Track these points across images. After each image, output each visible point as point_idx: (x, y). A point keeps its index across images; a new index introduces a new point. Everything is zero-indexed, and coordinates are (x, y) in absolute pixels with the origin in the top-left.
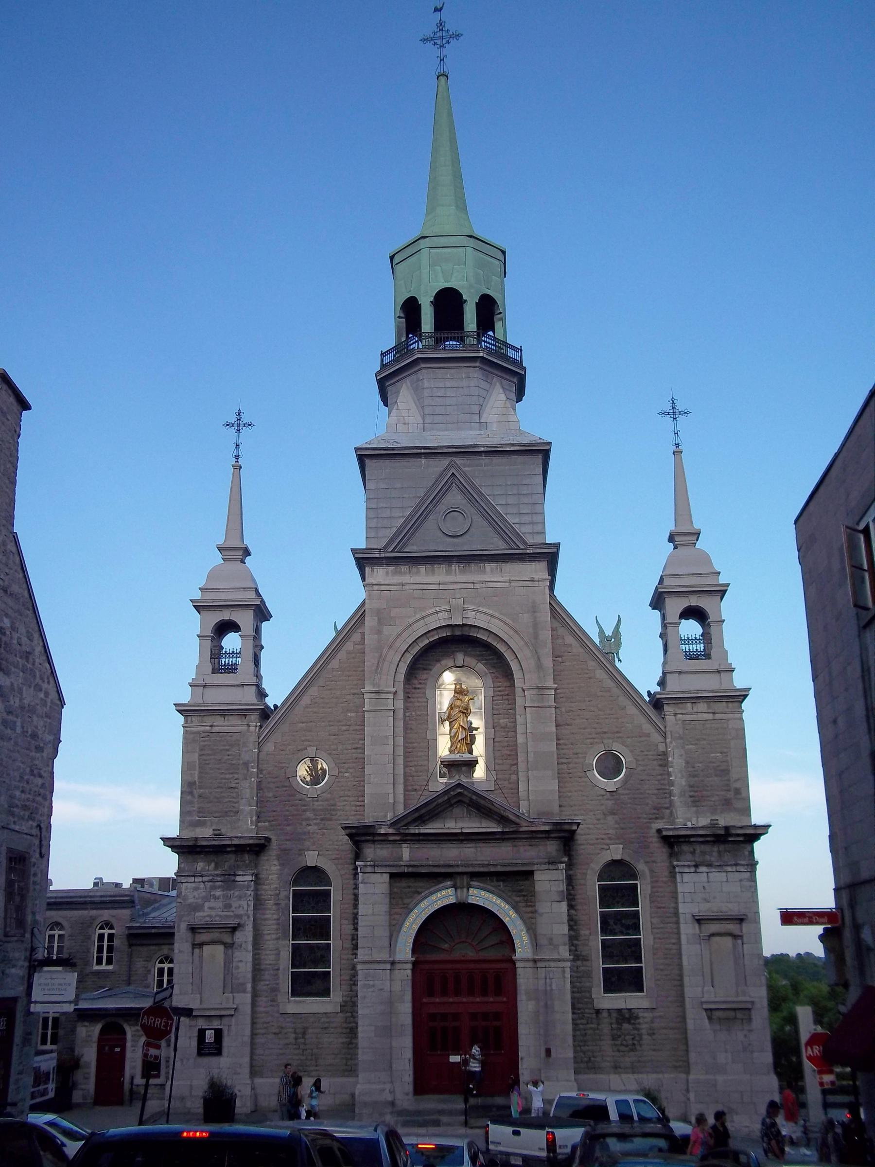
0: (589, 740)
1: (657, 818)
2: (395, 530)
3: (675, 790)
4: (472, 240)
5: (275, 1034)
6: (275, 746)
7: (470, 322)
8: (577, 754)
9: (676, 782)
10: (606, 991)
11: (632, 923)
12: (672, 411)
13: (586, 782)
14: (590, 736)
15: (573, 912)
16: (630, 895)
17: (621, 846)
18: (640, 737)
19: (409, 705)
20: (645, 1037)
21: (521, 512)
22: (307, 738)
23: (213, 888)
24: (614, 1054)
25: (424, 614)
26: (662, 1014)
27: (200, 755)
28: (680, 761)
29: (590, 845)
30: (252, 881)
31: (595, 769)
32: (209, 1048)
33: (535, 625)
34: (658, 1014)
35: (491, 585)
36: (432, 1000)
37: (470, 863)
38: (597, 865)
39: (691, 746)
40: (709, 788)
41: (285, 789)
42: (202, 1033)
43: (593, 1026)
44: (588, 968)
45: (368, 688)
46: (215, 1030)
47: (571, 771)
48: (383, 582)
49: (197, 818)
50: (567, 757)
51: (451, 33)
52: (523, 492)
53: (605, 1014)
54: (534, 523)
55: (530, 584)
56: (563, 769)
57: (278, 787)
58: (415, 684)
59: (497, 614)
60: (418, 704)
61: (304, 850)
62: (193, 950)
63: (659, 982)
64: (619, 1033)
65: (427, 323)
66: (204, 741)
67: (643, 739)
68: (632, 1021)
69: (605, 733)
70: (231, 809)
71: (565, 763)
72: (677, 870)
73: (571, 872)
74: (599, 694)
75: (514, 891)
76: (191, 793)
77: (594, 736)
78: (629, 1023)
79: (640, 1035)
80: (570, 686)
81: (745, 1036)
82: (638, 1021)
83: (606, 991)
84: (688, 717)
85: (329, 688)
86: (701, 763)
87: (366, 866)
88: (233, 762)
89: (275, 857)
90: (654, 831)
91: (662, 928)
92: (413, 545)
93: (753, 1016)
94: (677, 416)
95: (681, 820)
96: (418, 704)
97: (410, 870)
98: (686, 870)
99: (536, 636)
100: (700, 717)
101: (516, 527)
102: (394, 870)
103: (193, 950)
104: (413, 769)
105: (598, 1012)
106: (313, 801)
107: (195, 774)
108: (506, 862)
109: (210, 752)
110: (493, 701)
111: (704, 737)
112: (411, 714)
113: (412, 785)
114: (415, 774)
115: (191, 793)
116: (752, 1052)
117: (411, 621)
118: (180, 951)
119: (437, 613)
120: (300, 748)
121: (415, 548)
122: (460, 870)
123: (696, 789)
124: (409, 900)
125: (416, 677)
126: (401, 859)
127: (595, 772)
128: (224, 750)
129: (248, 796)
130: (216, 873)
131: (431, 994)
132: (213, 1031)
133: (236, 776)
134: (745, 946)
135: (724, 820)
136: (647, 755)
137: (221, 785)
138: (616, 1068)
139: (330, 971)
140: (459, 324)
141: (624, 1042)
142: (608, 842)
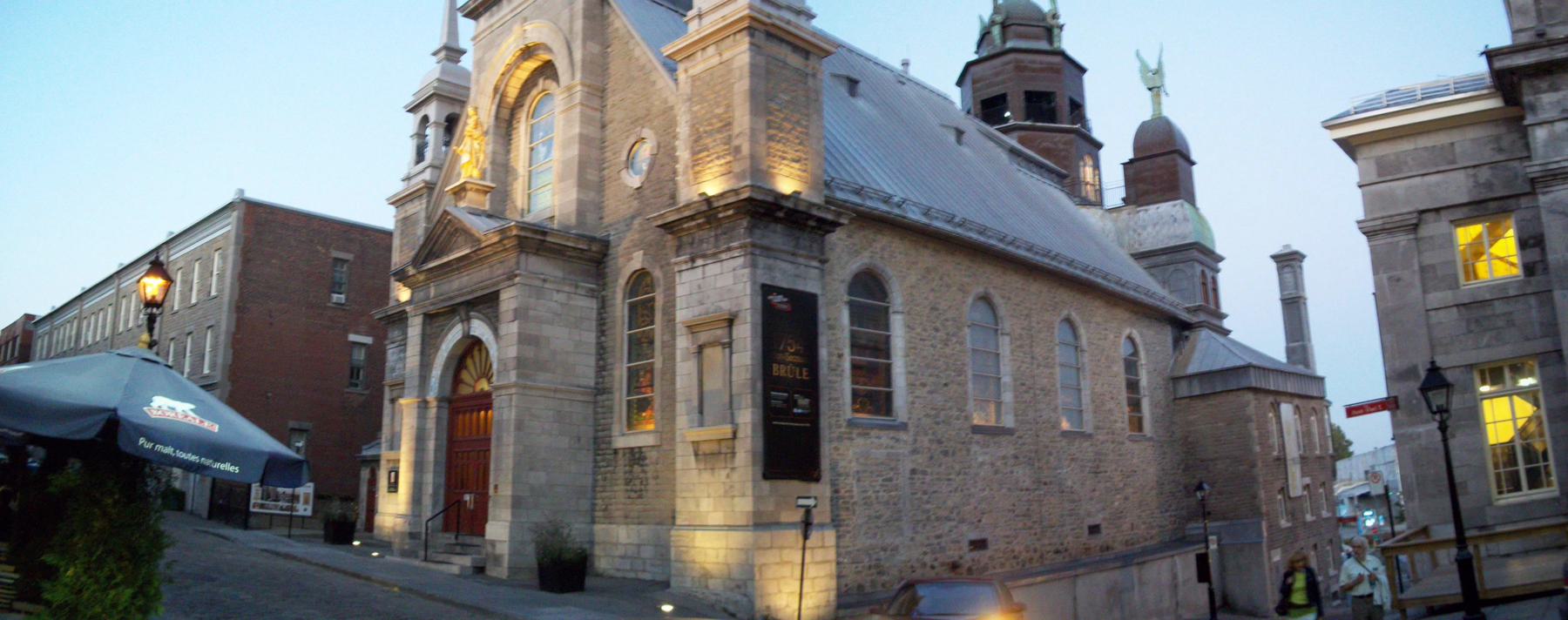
3: (680, 167)
15: (603, 339)
17: (641, 252)
20: (651, 481)
73: (603, 293)
78: (638, 464)
79: (647, 479)
81: (728, 476)
93: (737, 450)
98: (684, 267)
105: (616, 451)
116: (733, 497)
126: (428, 298)
134: (734, 356)
138: (627, 519)
141: (634, 488)
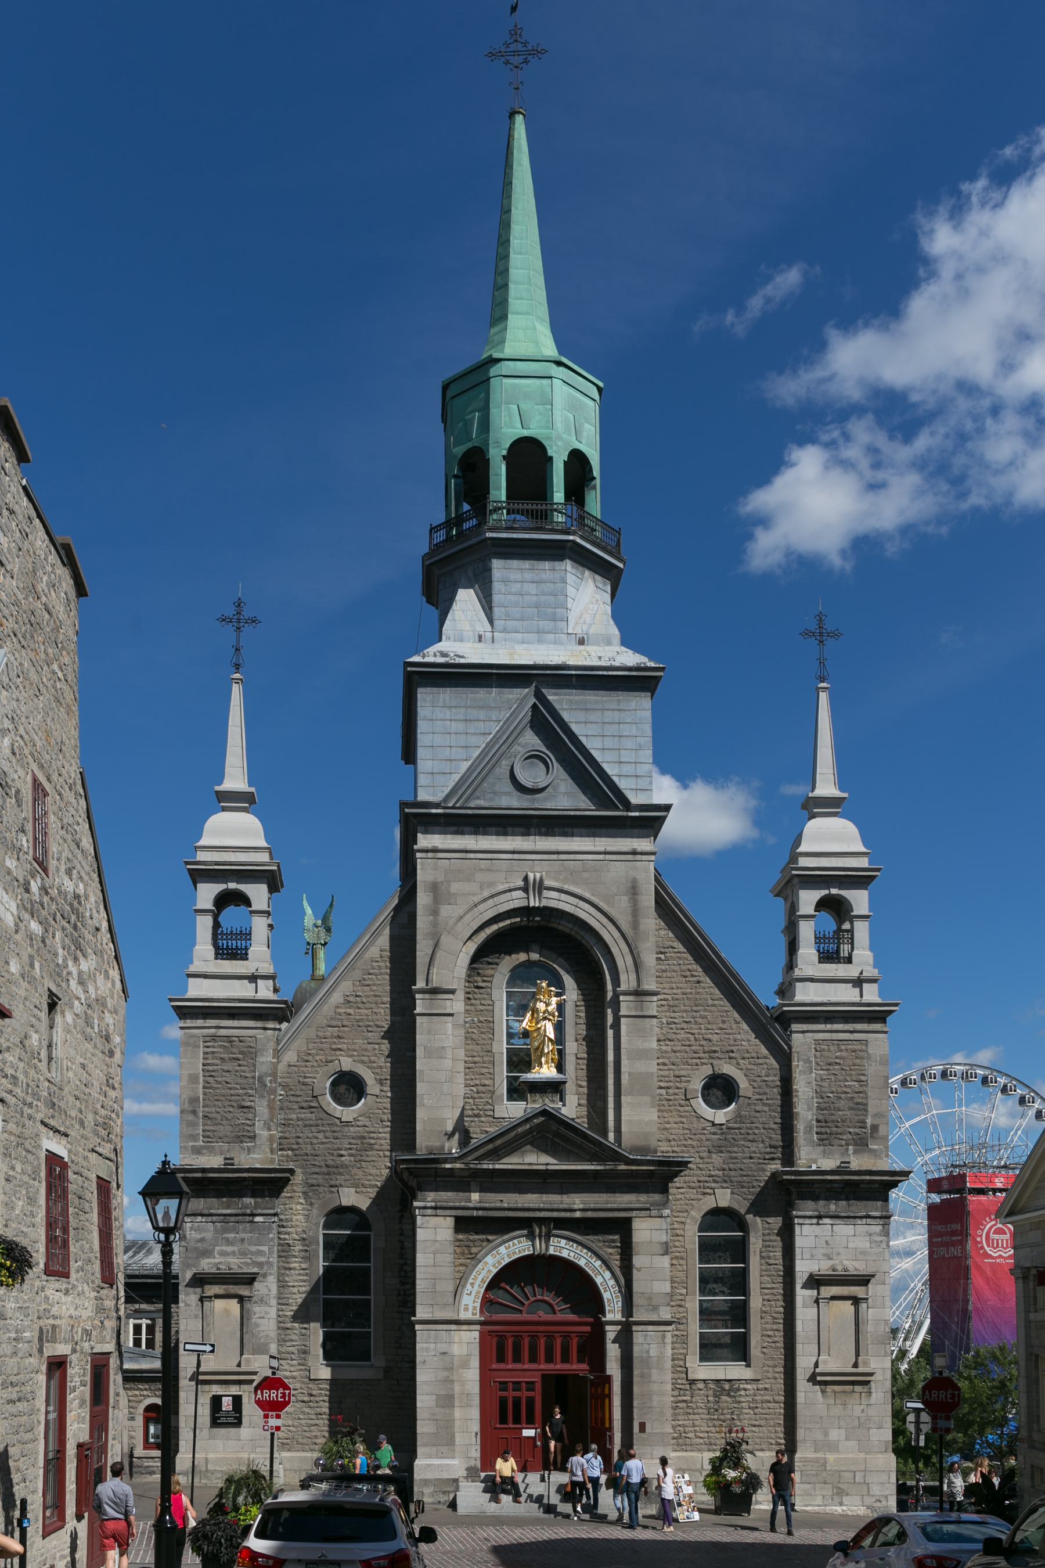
0: (694, 1060)
1: (773, 1159)
2: (456, 777)
4: (562, 369)
5: (303, 1402)
6: (298, 1056)
7: (559, 496)
8: (679, 1077)
9: (801, 1115)
10: (702, 1359)
11: (739, 1282)
12: (818, 631)
13: (688, 1112)
14: (696, 1055)
16: (739, 1250)
18: (758, 1058)
19: (468, 1008)
21: (622, 760)
22: (339, 1047)
23: (226, 1230)
24: (708, 1429)
25: (494, 891)
26: (767, 1386)
27: (204, 1065)
28: (807, 1089)
29: (690, 1187)
30: (274, 1222)
31: (700, 1095)
32: (226, 1417)
33: (635, 912)
34: (761, 1386)
35: (581, 857)
36: (502, 1366)
37: (555, 1206)
38: (697, 1215)
39: (821, 1072)
40: (839, 1124)
41: (312, 1110)
42: (216, 1401)
43: (685, 1398)
44: (682, 1333)
45: (420, 984)
46: (234, 1397)
47: (670, 1097)
48: (441, 846)
49: (202, 1143)
50: (667, 1079)
51: (530, 47)
52: (625, 734)
53: (701, 1385)
54: (637, 776)
55: (630, 857)
56: (661, 1095)
57: (302, 1108)
58: (477, 982)
59: (587, 895)
60: (482, 1008)
61: (337, 1186)
62: (202, 1303)
63: (765, 1350)
64: (716, 1407)
65: (499, 490)
66: (208, 1047)
67: (760, 1061)
68: (732, 1394)
69: (715, 1052)
70: (244, 1133)
71: (663, 1088)
72: (796, 1221)
74: (710, 1002)
75: (604, 1241)
76: (194, 1112)
77: (702, 1055)
78: (729, 1395)
80: (675, 991)
81: (863, 1411)
82: (739, 1393)
83: (702, 1359)
84: (821, 1036)
85: (366, 983)
86: (832, 1093)
87: (425, 1208)
88: (247, 1075)
89: (301, 1194)
90: (769, 1174)
91: (773, 1288)
92: (478, 798)
93: (872, 1390)
94: (824, 638)
95: (804, 1161)
96: (482, 1008)
97: (481, 1213)
98: (807, 1221)
99: (635, 925)
100: (835, 1036)
101: (615, 779)
102: (460, 1213)
103: (202, 1303)
104: (474, 1089)
105: (693, 1382)
106: (348, 1126)
107: (197, 1088)
108: (598, 1206)
109: (215, 1061)
110: (577, 1006)
111: (838, 1061)
112: (473, 1020)
113: (473, 1109)
114: (476, 1095)
115: (194, 1112)
117: (477, 899)
118: (186, 1305)
119: (510, 890)
120: (330, 1058)
121: (481, 803)
122: (542, 1214)
123: (824, 1124)
124: (480, 1248)
125: (478, 974)
127: (700, 1100)
128: (234, 1058)
129: (266, 1116)
130: (228, 1211)
131: (501, 1359)
132: (231, 1398)
133: (250, 1091)
135: (857, 1162)
136: (765, 1081)
137: (232, 1103)
139: (370, 1332)
140: (543, 492)
141: (722, 1417)
142: (713, 1185)
